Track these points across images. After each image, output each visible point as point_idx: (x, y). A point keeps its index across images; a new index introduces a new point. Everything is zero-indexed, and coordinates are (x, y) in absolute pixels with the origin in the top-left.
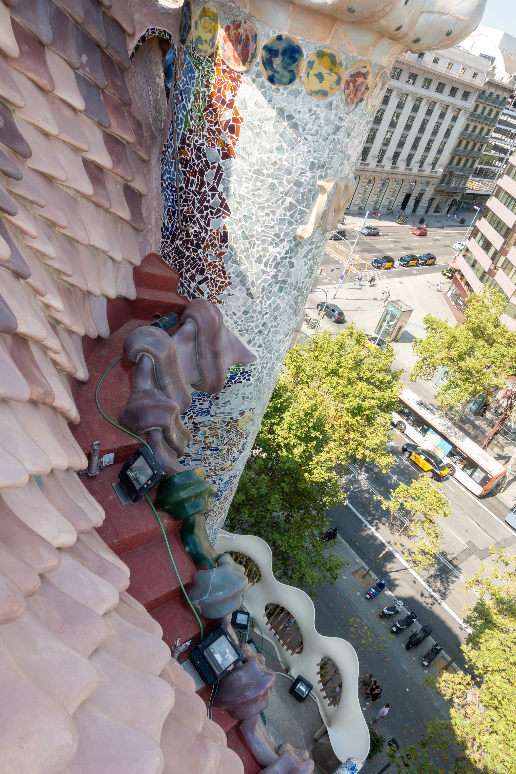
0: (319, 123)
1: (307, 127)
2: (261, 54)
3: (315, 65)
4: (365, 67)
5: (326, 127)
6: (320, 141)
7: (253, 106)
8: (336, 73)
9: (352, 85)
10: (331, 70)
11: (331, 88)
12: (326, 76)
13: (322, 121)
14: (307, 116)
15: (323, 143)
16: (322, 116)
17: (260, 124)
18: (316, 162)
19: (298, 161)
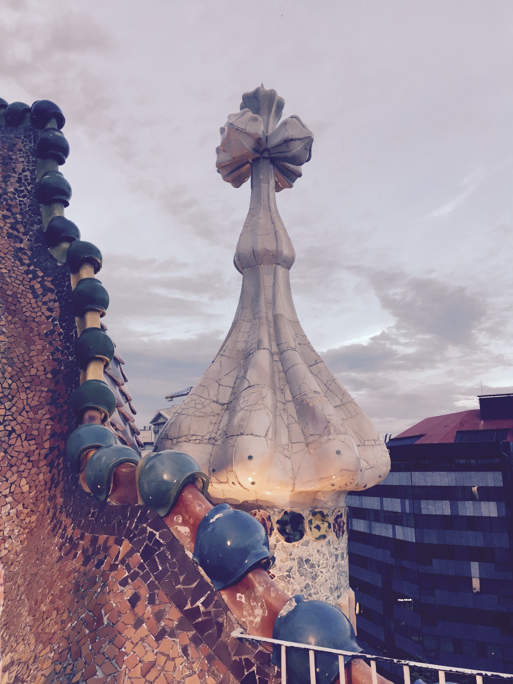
0: (326, 558)
1: (320, 564)
2: (276, 526)
3: (313, 522)
4: (339, 511)
5: (331, 559)
6: (331, 570)
7: (280, 563)
8: (326, 522)
9: (336, 525)
10: (323, 521)
11: (327, 532)
12: (321, 525)
13: (328, 555)
14: (318, 556)
15: (333, 571)
16: (326, 552)
17: (288, 573)
18: (332, 586)
19: (322, 590)
